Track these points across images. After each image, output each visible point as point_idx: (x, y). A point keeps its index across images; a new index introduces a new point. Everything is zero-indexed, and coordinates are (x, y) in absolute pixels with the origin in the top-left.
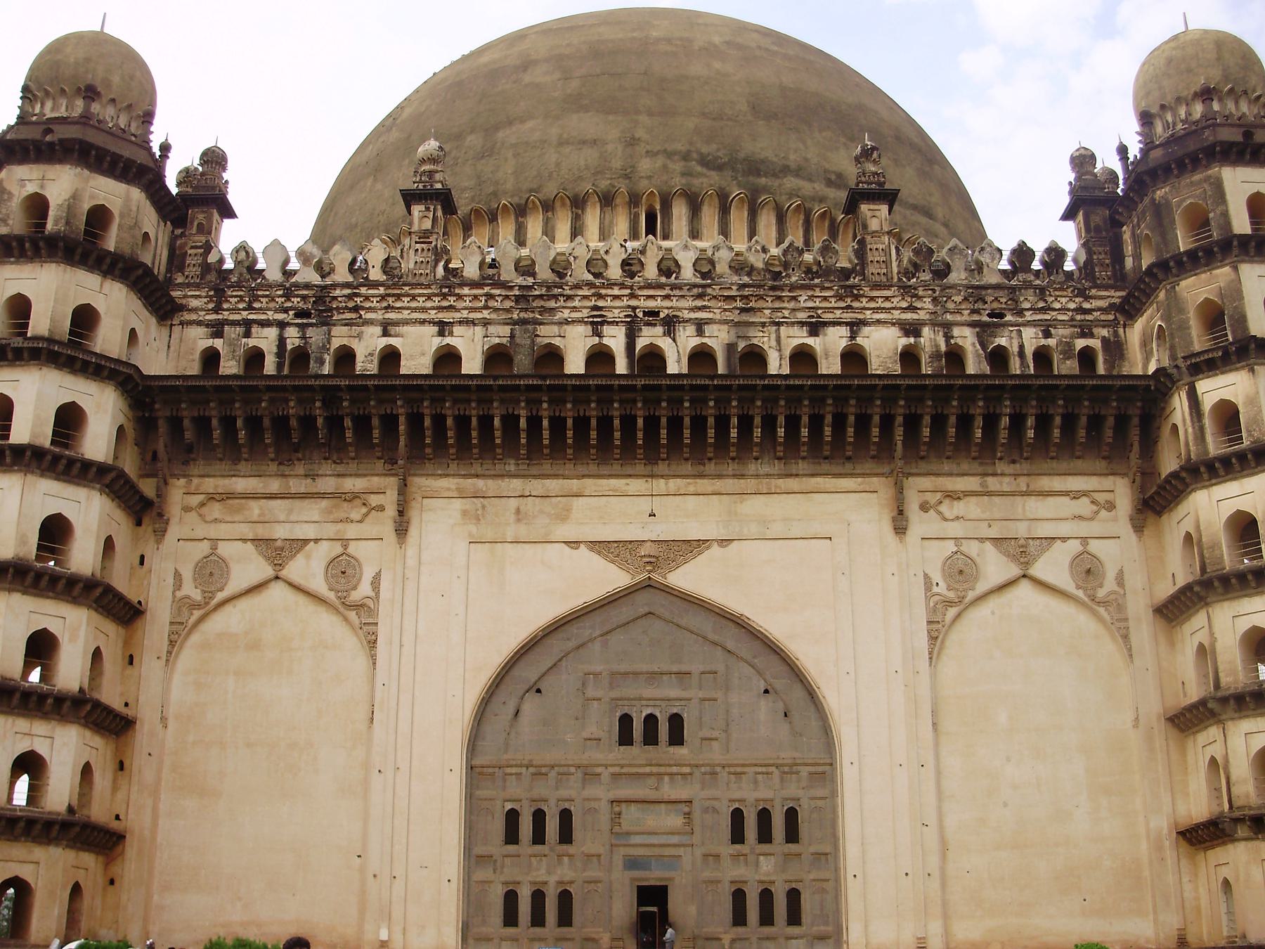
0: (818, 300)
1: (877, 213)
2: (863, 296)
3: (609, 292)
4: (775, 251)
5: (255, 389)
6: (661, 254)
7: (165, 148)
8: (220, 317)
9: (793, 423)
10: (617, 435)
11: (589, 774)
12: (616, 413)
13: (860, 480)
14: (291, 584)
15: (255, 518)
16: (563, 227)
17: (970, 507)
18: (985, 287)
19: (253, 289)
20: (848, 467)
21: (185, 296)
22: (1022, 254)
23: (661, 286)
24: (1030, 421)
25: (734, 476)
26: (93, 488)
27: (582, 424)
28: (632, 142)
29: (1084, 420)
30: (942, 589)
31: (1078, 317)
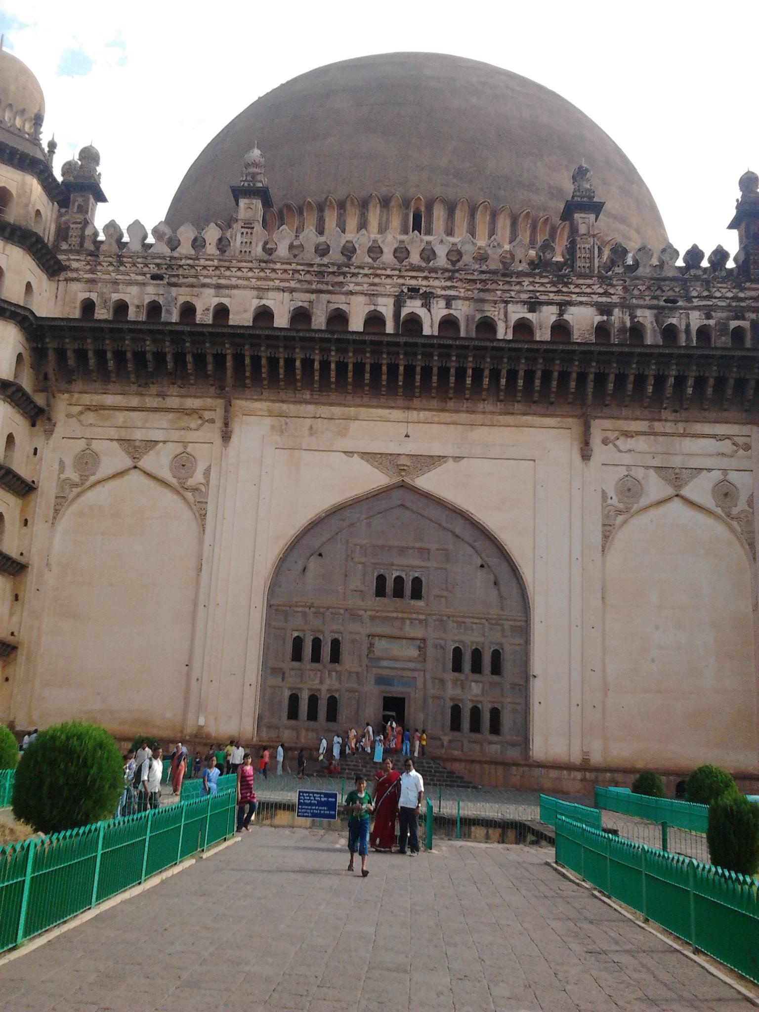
0: (537, 285)
1: (587, 221)
2: (571, 283)
3: (383, 272)
4: (507, 247)
5: (120, 330)
6: (423, 245)
8: (95, 276)
9: (512, 376)
10: (384, 377)
12: (385, 362)
13: (559, 419)
14: (145, 472)
15: (120, 424)
16: (352, 222)
17: (640, 444)
18: (663, 279)
19: (120, 256)
20: (551, 408)
21: (69, 260)
22: (695, 254)
23: (420, 269)
24: (690, 382)
25: (468, 412)
27: (359, 368)
29: (732, 382)
30: (615, 501)
31: (734, 304)
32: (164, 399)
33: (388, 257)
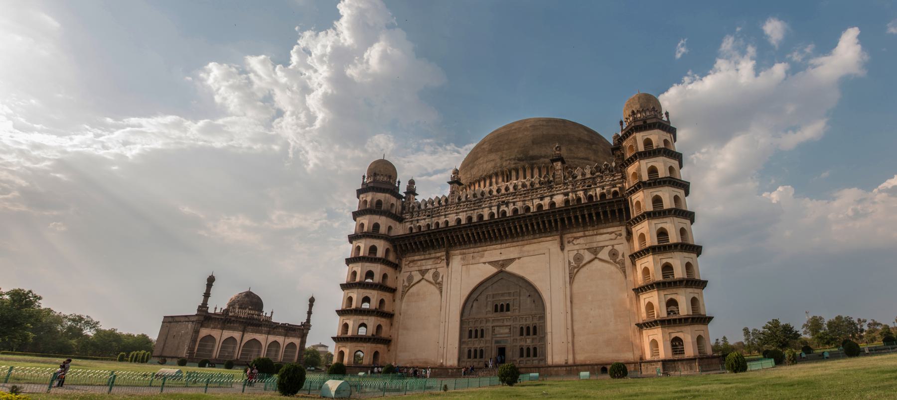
7: (399, 182)
11: (487, 321)
17: (581, 241)
28: (502, 158)
30: (573, 264)
33: (495, 193)
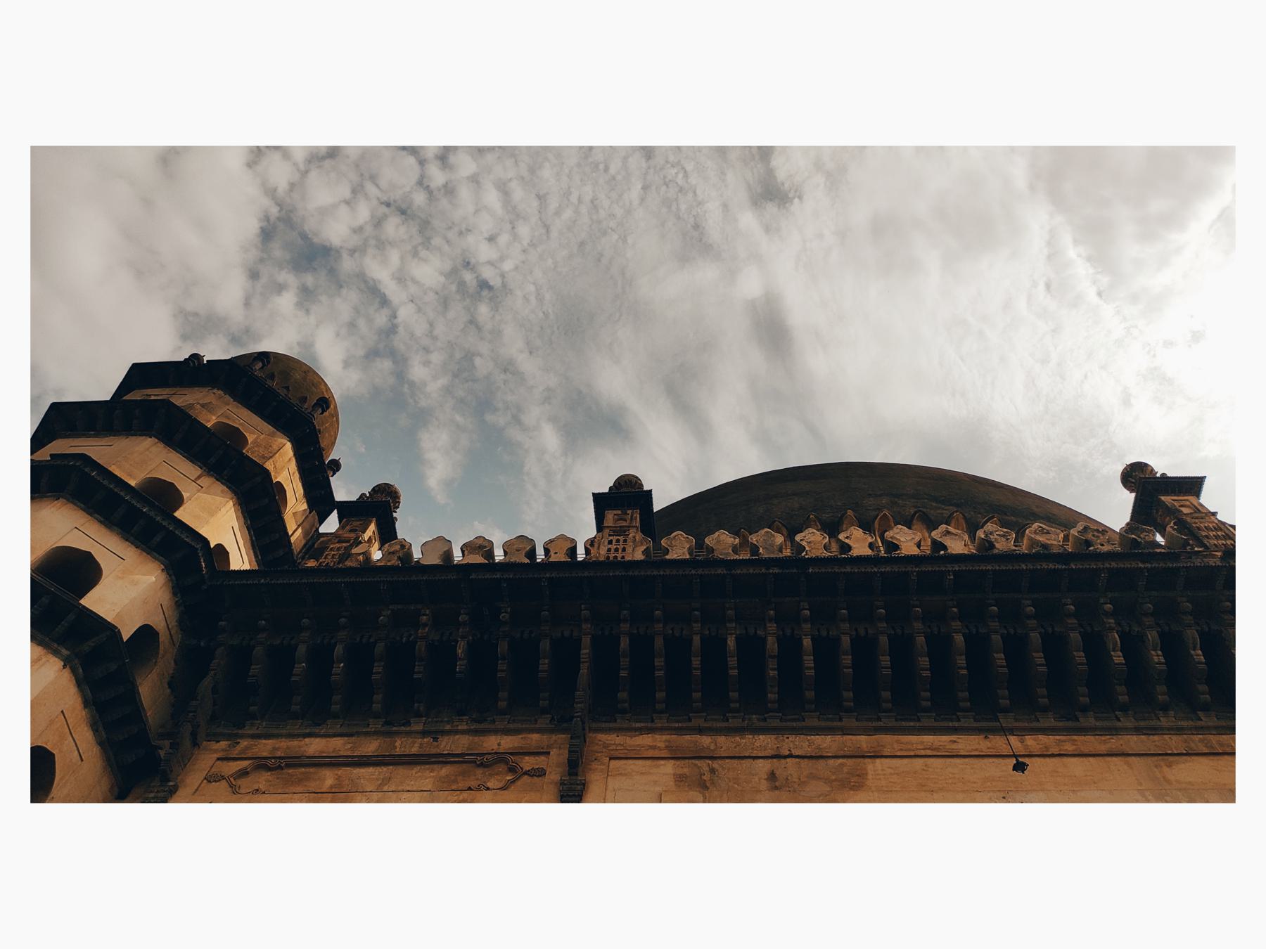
25: (1138, 731)
26: (56, 653)
32: (435, 739)
